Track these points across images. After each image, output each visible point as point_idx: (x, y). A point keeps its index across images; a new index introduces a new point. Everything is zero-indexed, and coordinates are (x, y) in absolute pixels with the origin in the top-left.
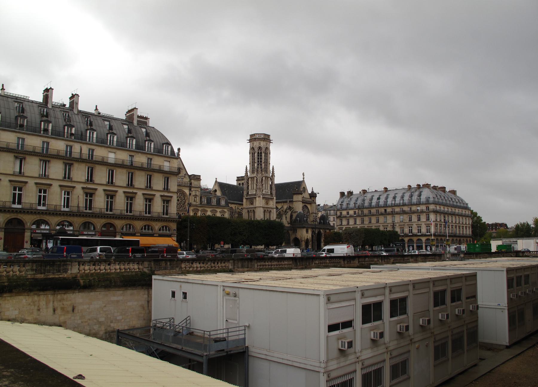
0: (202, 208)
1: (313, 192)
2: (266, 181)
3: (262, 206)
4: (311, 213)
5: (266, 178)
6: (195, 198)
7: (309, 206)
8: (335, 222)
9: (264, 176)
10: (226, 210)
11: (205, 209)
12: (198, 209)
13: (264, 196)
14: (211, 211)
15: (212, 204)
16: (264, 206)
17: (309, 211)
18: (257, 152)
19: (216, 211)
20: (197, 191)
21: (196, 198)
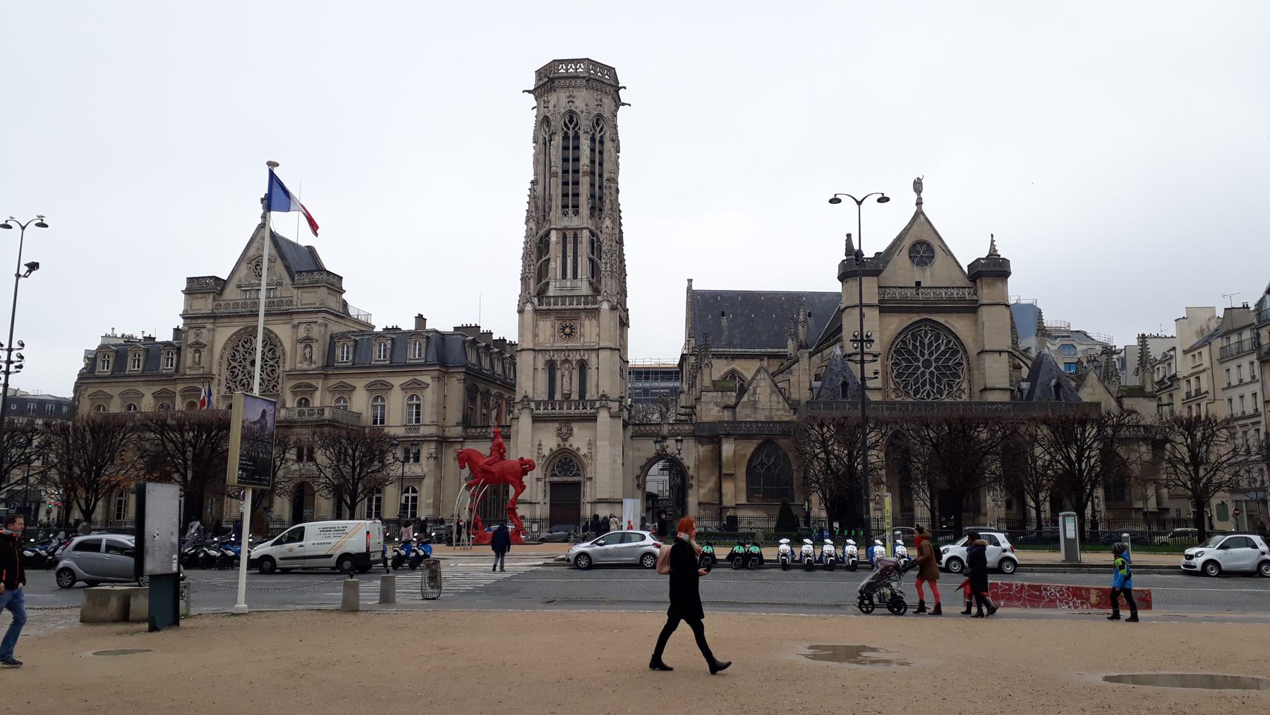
0: (333, 382)
1: (993, 254)
2: (570, 247)
3: (531, 346)
4: (978, 354)
5: (570, 235)
6: (305, 347)
7: (959, 325)
8: (1256, 387)
9: (551, 227)
10: (426, 379)
11: (344, 380)
12: (309, 386)
13: (544, 307)
14: (369, 388)
15: (372, 363)
16: (548, 346)
17: (962, 344)
18: (541, 139)
19: (389, 387)
20: (312, 325)
21: (311, 347)
